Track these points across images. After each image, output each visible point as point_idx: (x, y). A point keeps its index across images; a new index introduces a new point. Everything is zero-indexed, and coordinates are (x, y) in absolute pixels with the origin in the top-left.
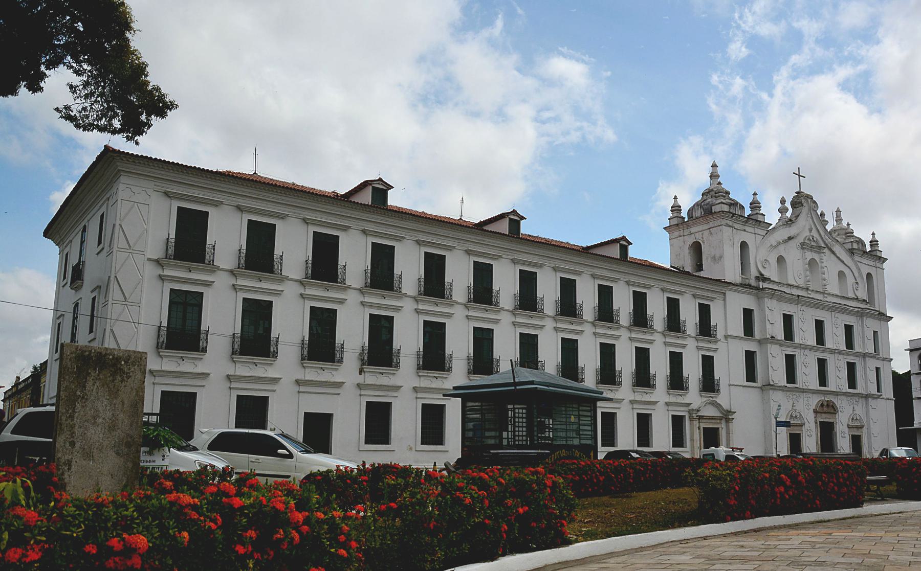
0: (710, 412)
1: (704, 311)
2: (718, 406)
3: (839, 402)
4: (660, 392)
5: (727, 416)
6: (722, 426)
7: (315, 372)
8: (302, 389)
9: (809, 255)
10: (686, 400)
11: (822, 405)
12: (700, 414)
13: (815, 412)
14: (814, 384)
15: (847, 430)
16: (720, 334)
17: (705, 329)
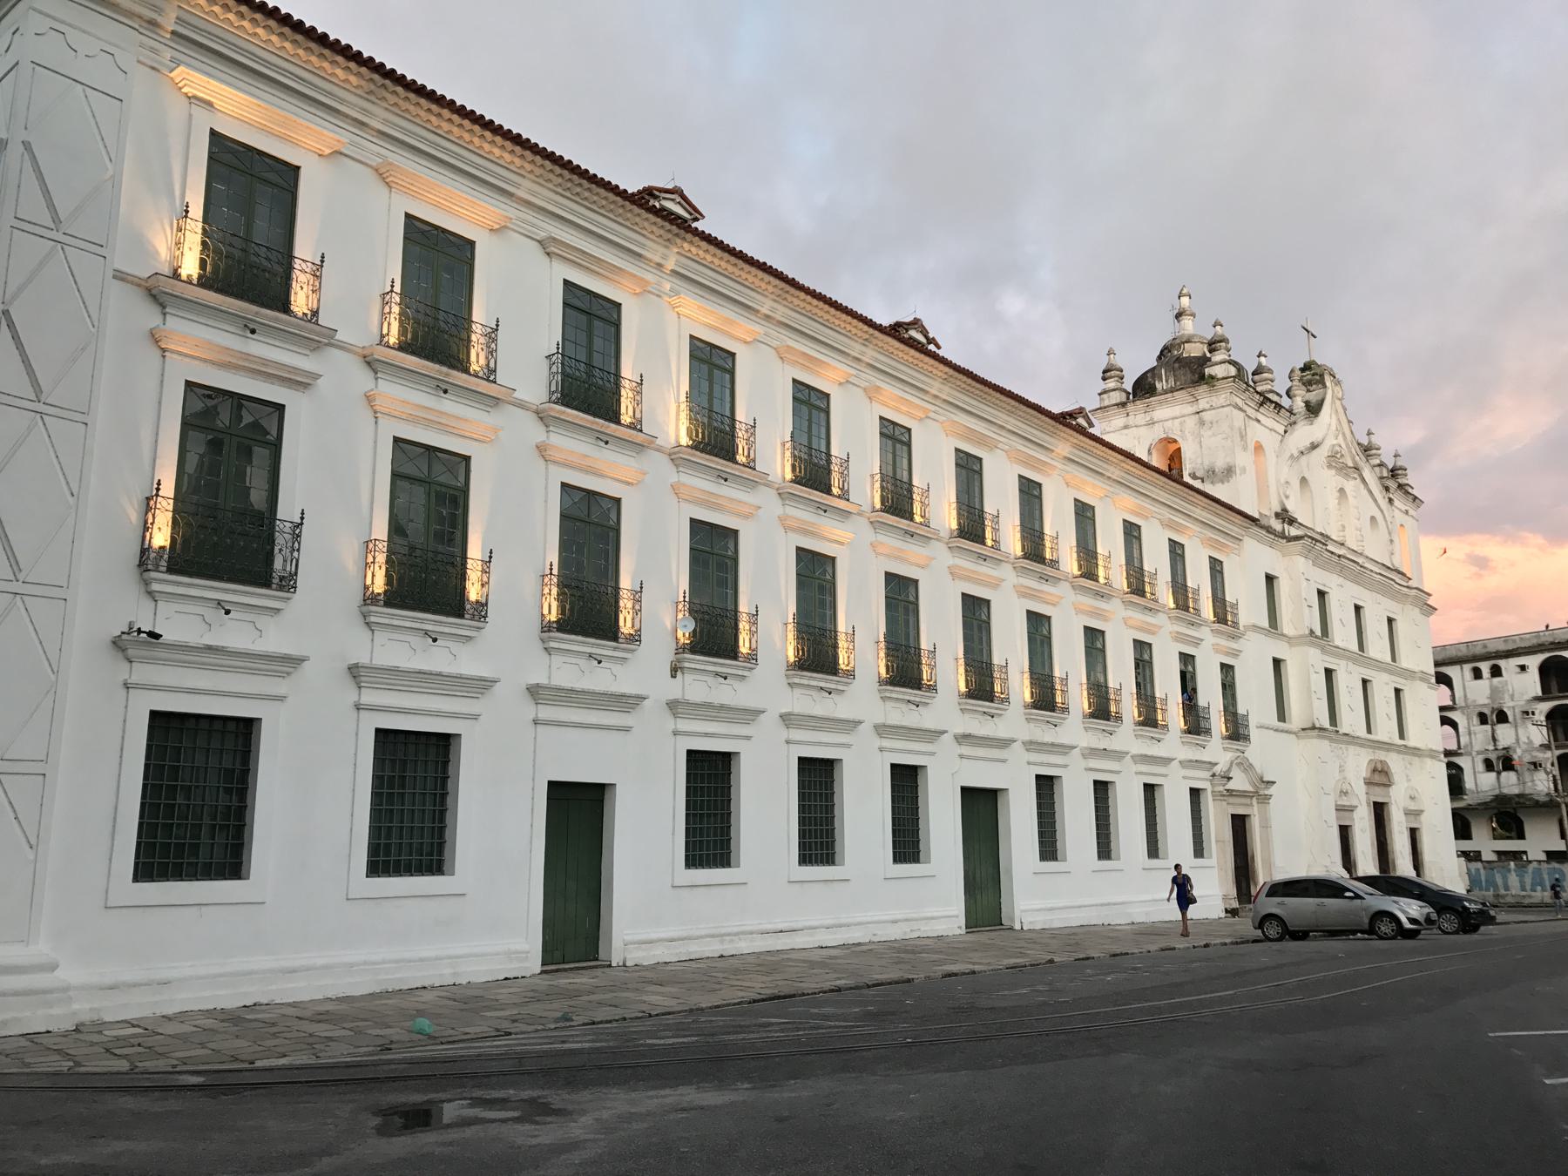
0: (1239, 782)
1: (1216, 567)
2: (1247, 767)
3: (1395, 762)
4: (1074, 728)
5: (1261, 789)
6: (1254, 811)
7: (574, 666)
8: (546, 712)
9: (1339, 481)
10: (1205, 756)
11: (1375, 770)
12: (1231, 785)
13: (1368, 783)
14: (1362, 732)
15: (1403, 818)
16: (1243, 620)
17: (1223, 612)
